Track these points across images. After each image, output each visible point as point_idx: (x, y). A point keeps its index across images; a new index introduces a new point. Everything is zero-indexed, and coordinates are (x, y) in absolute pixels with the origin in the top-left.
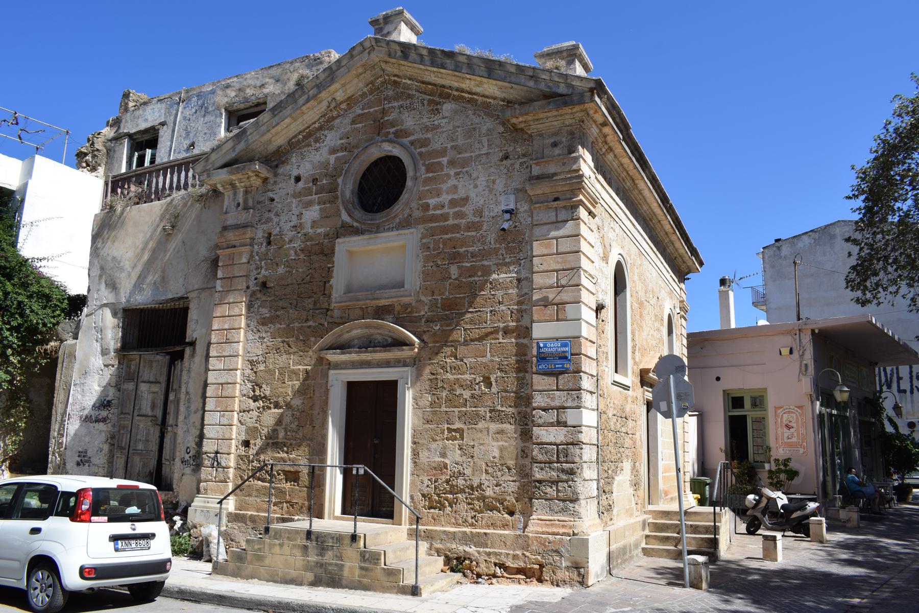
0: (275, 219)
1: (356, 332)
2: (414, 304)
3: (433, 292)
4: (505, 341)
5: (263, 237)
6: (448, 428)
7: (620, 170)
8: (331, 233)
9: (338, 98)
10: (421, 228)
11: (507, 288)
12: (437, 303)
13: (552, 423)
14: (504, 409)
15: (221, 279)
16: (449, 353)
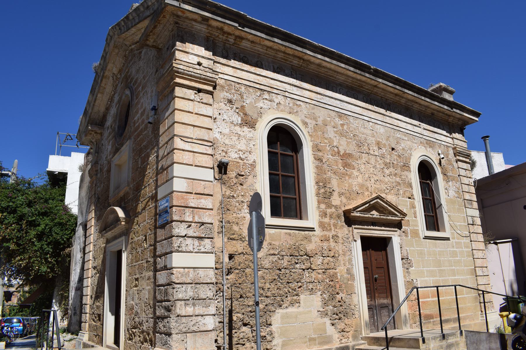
7: (271, 53)
9: (115, 72)
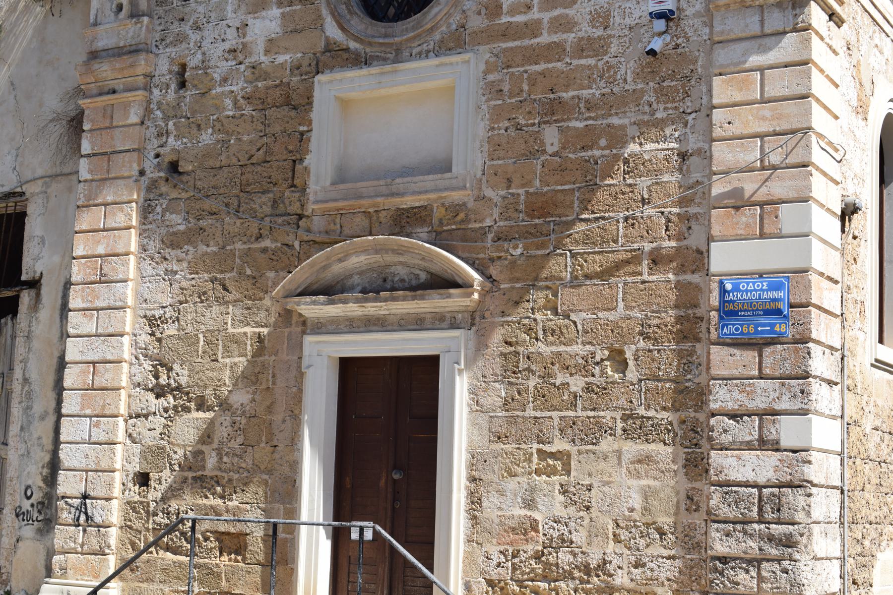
0: (194, 37)
1: (357, 261)
2: (471, 204)
3: (509, 180)
4: (654, 278)
5: (170, 72)
6: (539, 451)
8: (305, 63)
10: (485, 52)
11: (658, 172)
12: (517, 203)
13: (748, 442)
14: (651, 413)
15: (88, 156)
16: (541, 302)
